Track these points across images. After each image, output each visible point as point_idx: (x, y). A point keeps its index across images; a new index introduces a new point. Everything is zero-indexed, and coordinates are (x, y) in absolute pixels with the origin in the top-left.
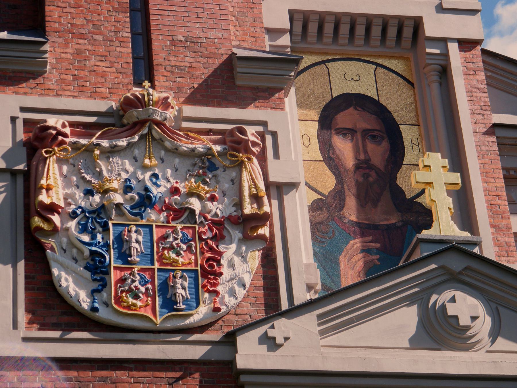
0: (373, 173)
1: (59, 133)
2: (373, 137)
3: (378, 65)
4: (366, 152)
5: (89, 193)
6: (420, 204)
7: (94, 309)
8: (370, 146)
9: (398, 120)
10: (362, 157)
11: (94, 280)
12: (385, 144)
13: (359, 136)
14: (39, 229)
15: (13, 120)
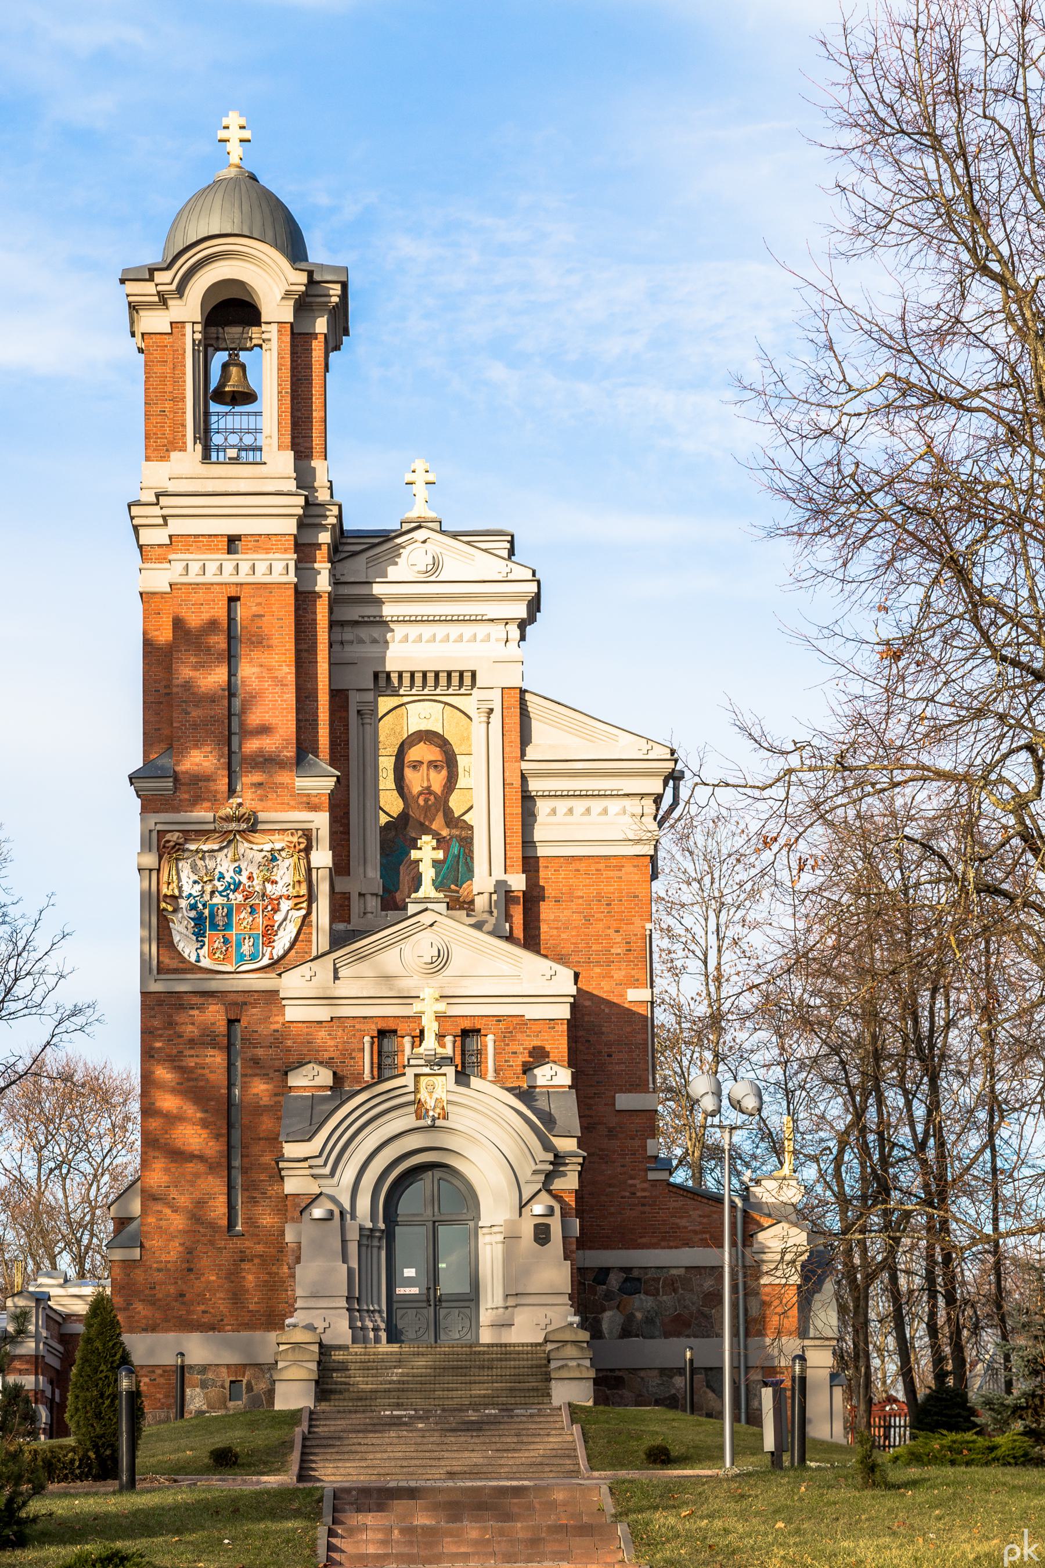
0: (432, 798)
1: (177, 844)
2: (436, 767)
3: (446, 704)
4: (428, 780)
5: (195, 882)
6: (464, 821)
7: (198, 961)
8: (433, 773)
9: (457, 751)
10: (425, 785)
11: (198, 941)
12: (444, 772)
13: (425, 766)
14: (165, 910)
15: (150, 831)
